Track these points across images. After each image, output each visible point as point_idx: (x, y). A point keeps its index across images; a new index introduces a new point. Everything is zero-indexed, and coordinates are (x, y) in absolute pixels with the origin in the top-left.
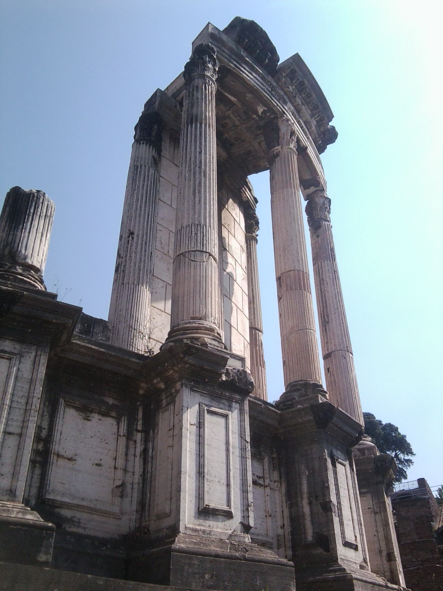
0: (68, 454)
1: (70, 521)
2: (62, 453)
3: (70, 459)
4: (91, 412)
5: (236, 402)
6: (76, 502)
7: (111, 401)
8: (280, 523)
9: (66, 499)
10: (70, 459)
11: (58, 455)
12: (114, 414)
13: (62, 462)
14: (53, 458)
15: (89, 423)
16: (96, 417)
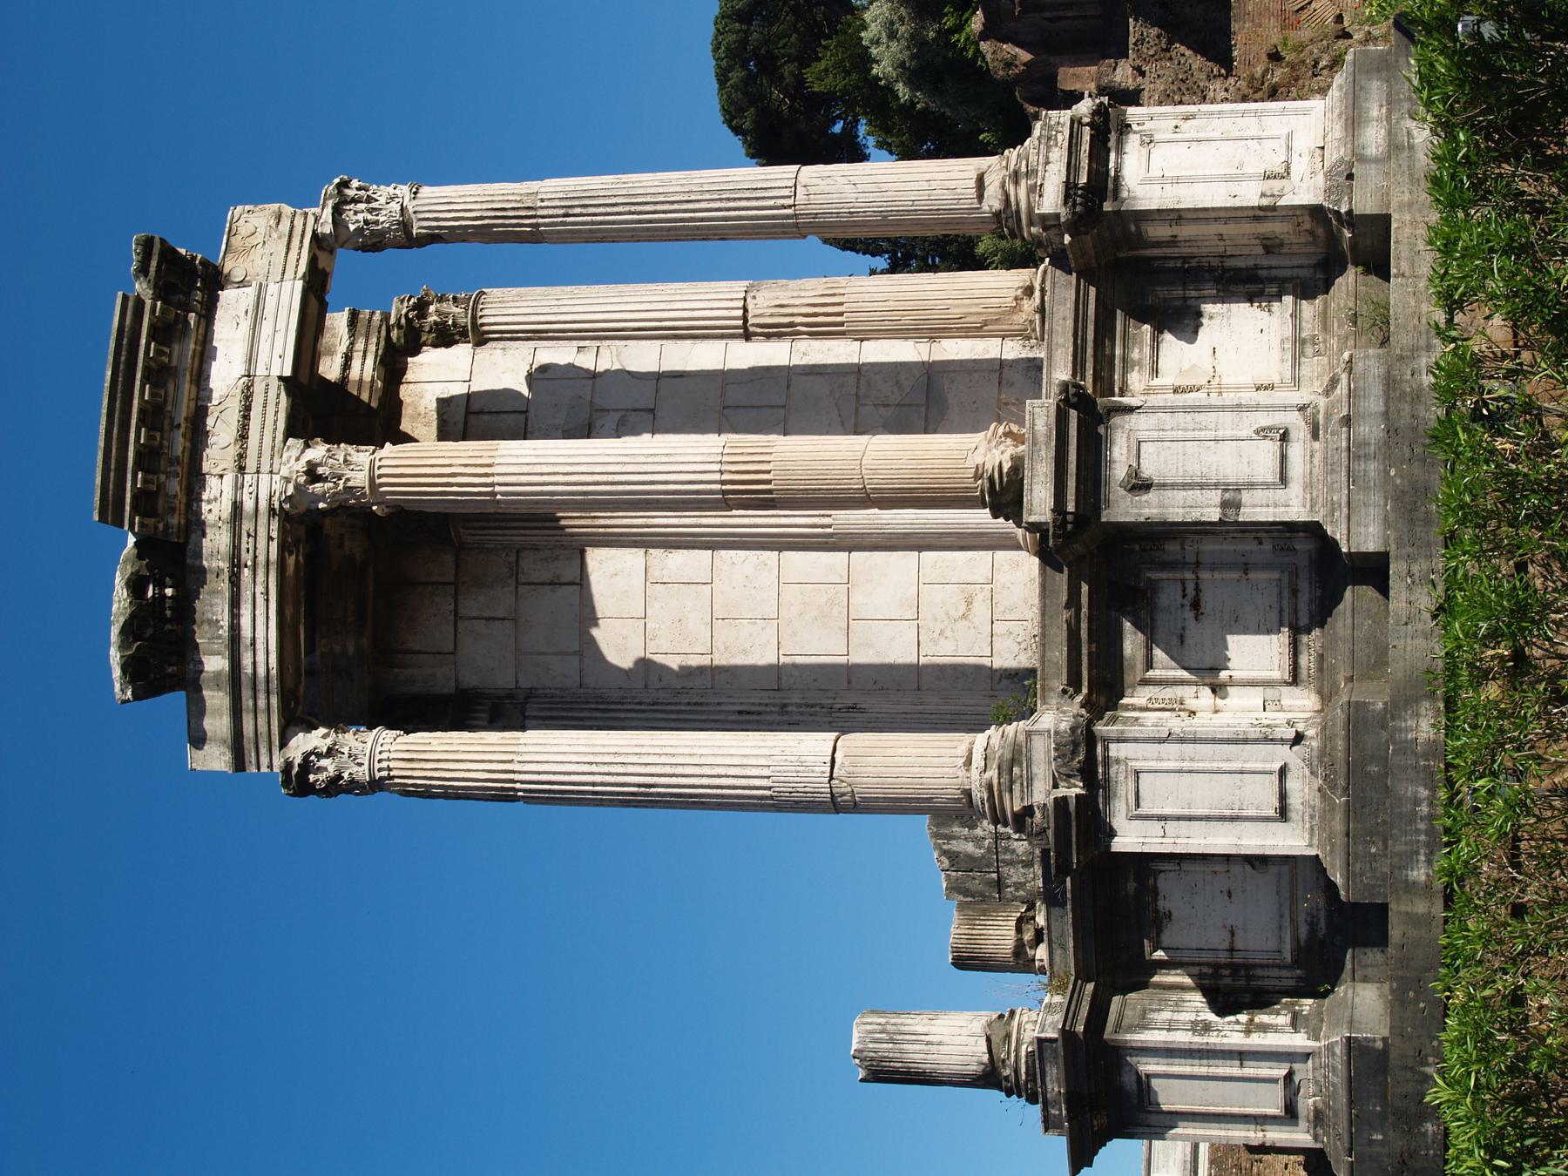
0: (1227, 936)
1: (1313, 926)
2: (1226, 945)
3: (1233, 934)
4: (1157, 911)
5: (1106, 749)
6: (1287, 923)
7: (1132, 886)
8: (1254, 546)
9: (1288, 938)
10: (1233, 934)
11: (1232, 950)
12: (1151, 881)
13: (1239, 945)
14: (1238, 958)
15: (1175, 914)
16: (1161, 903)
